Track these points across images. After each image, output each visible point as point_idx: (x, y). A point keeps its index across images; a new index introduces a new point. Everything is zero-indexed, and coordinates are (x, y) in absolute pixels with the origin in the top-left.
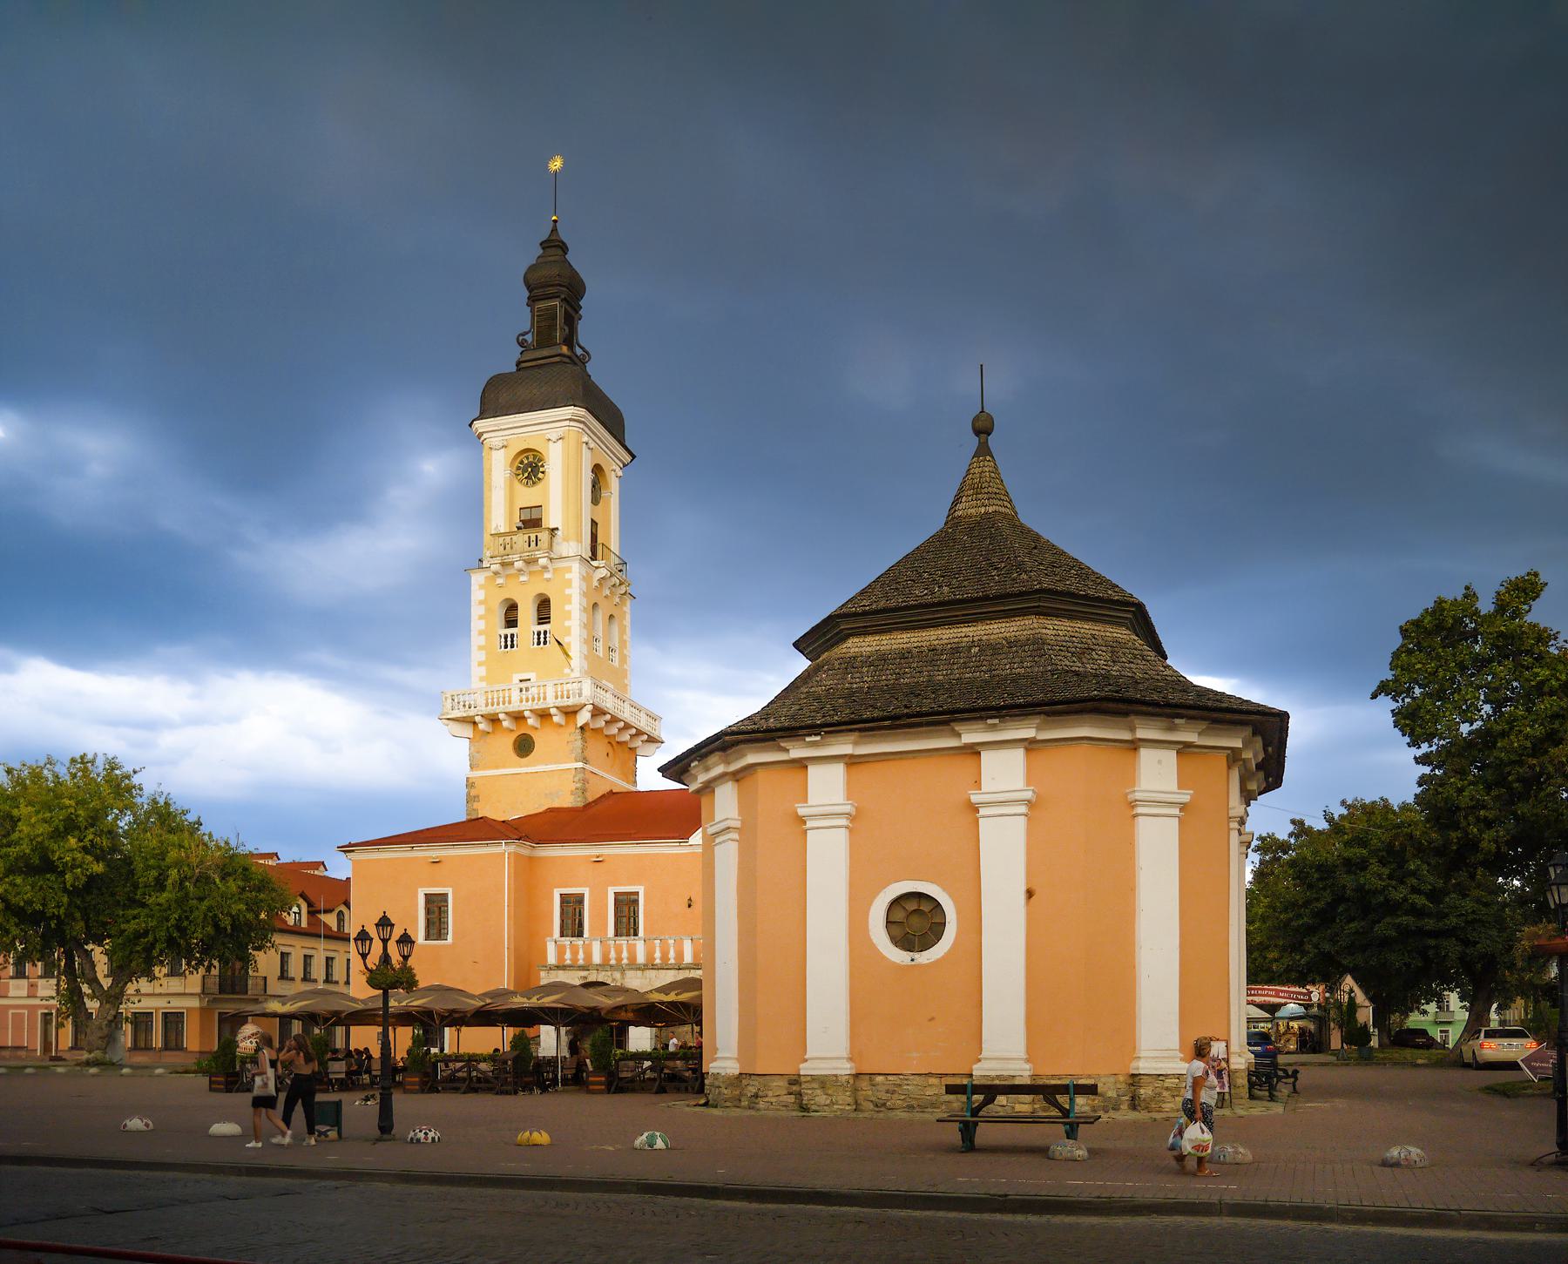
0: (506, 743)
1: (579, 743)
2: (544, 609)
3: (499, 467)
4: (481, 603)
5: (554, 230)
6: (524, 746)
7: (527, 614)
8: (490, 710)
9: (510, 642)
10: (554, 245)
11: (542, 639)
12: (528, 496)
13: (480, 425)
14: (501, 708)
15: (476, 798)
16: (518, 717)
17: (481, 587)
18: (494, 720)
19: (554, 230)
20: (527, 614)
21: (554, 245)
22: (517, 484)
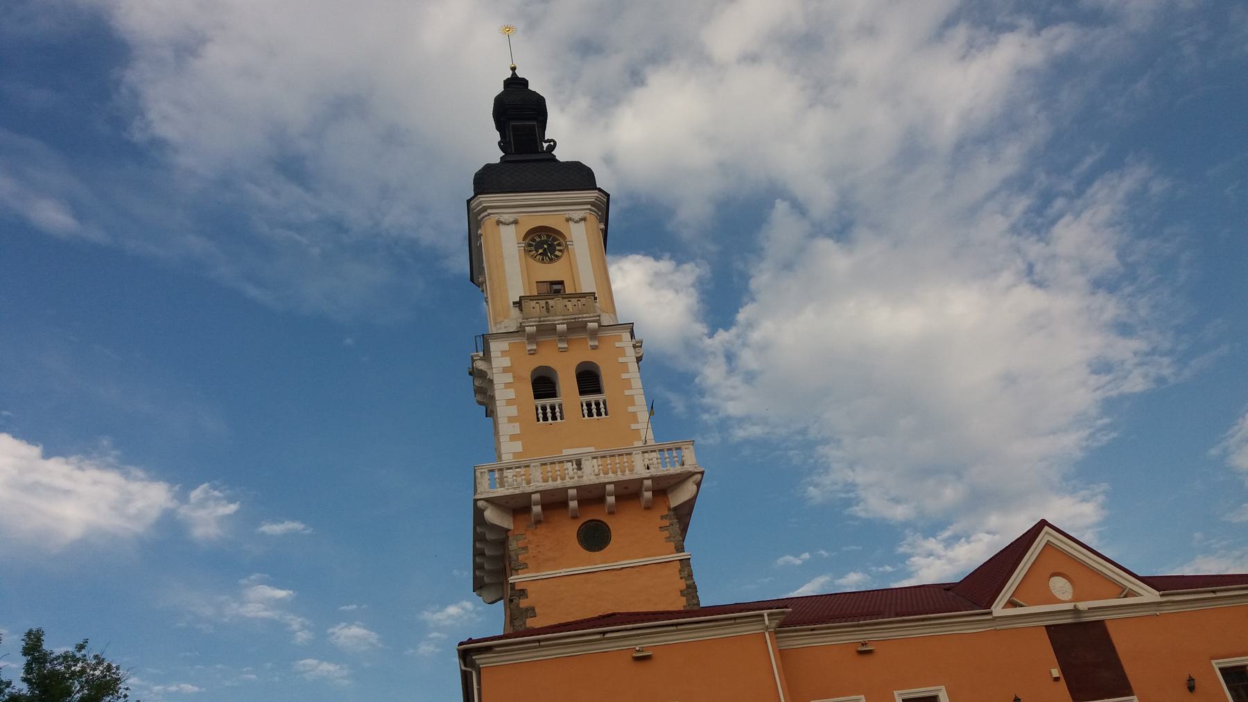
1: (676, 527)
2: (589, 380)
4: (506, 370)
5: (514, 74)
6: (595, 537)
7: (567, 384)
8: (551, 485)
11: (592, 410)
12: (551, 272)
13: (486, 199)
14: (568, 483)
15: (531, 611)
16: (592, 496)
17: (504, 353)
18: (555, 502)
19: (514, 74)
20: (567, 384)
22: (531, 261)
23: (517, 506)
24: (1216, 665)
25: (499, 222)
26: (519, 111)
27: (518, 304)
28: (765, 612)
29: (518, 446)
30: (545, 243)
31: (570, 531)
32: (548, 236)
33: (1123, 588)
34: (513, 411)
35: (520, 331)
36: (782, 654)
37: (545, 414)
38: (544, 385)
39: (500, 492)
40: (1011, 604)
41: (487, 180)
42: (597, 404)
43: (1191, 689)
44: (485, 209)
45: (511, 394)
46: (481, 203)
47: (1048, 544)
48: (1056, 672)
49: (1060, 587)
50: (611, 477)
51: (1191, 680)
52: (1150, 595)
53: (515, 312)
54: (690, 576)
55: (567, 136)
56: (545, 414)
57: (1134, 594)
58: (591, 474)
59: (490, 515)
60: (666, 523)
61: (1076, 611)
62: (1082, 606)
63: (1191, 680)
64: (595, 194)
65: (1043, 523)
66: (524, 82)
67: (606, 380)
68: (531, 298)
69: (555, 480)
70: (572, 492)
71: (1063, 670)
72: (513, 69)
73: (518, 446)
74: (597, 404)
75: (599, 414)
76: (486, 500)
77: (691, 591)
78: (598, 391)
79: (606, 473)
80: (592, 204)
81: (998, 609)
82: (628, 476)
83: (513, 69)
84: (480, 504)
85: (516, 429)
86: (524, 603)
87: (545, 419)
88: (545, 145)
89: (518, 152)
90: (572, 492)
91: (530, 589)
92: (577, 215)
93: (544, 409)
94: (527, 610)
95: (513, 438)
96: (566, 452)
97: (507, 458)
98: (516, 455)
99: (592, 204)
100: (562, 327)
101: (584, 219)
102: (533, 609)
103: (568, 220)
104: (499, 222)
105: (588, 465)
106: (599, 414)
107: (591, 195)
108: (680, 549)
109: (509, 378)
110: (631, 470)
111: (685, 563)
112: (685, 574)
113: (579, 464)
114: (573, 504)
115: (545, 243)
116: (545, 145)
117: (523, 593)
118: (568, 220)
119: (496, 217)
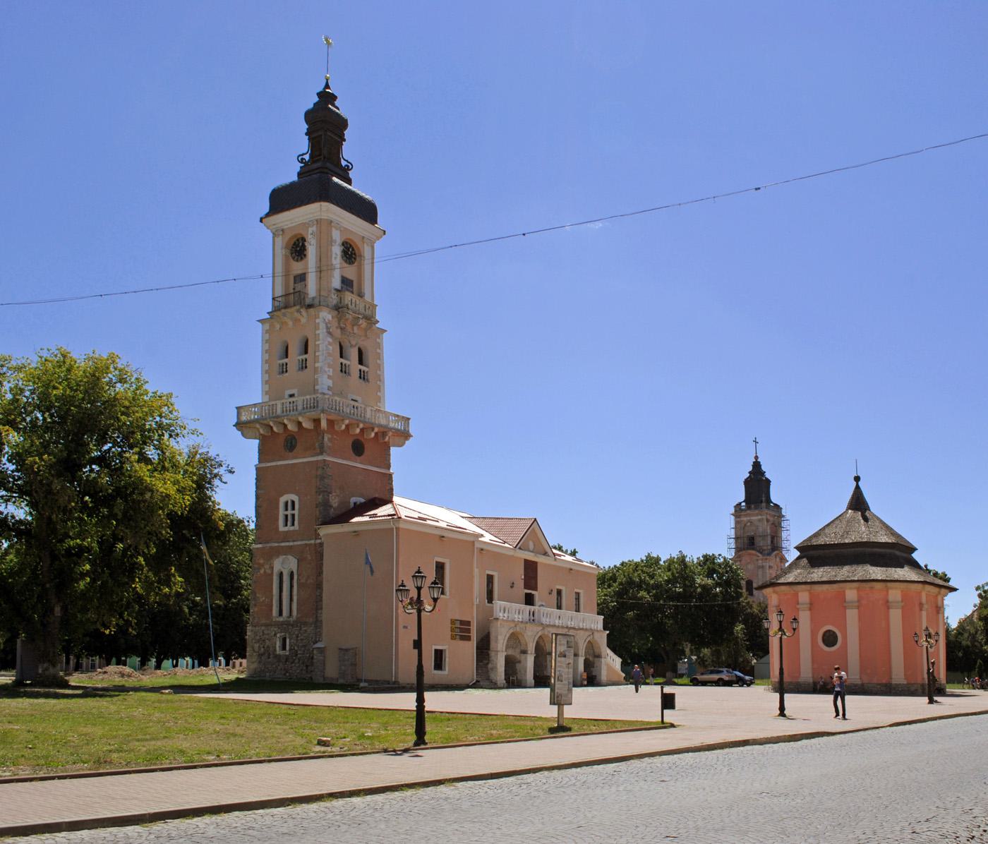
5: (327, 86)
10: (326, 97)
12: (350, 272)
19: (327, 86)
21: (326, 97)
29: (330, 383)
31: (349, 442)
66: (333, 98)
67: (369, 357)
73: (330, 383)
95: (329, 377)
98: (329, 388)
116: (344, 163)
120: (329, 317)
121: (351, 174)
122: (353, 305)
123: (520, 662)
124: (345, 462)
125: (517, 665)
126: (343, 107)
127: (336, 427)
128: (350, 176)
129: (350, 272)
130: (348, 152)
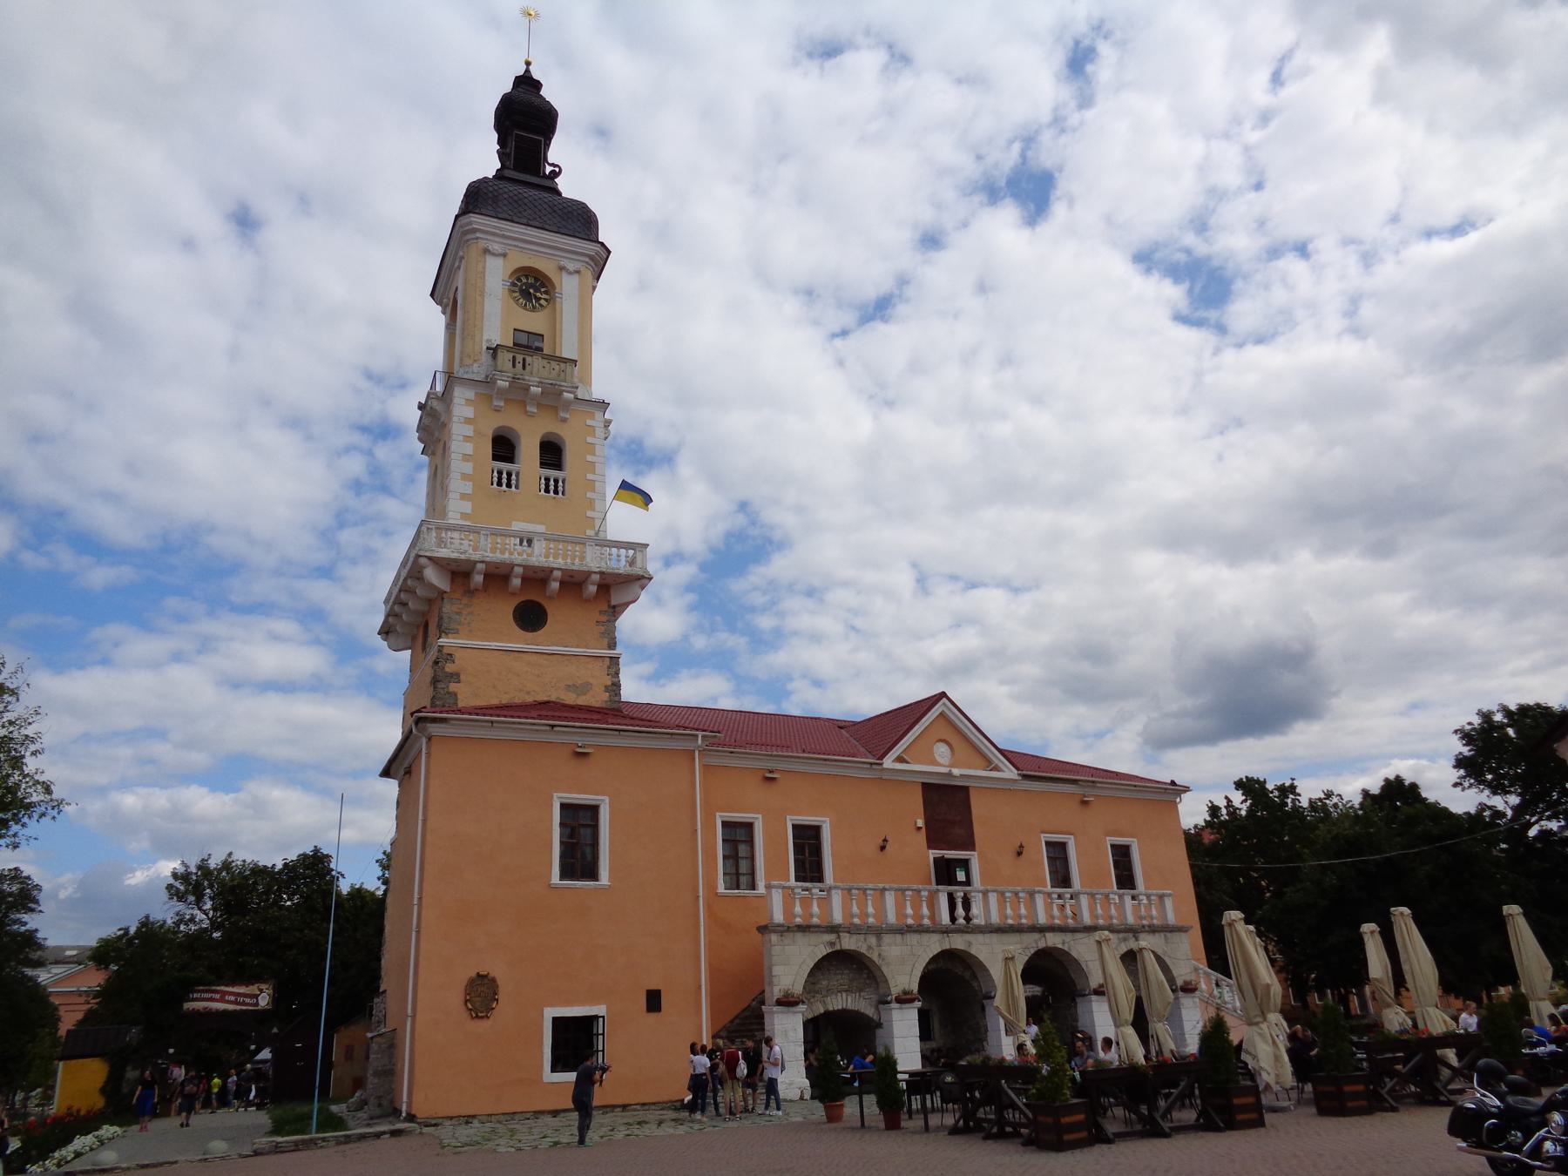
0: (505, 610)
2: (552, 453)
3: (495, 275)
4: (468, 421)
5: (527, 71)
6: (530, 617)
7: (529, 452)
8: (497, 557)
9: (506, 481)
10: (527, 83)
11: (553, 487)
12: (533, 321)
13: (476, 220)
14: (517, 559)
16: (537, 578)
19: (527, 71)
20: (529, 452)
21: (527, 83)
23: (459, 572)
24: (1044, 837)
25: (486, 251)
26: (525, 119)
27: (494, 351)
28: (700, 734)
29: (467, 507)
30: (532, 287)
31: (506, 609)
32: (536, 279)
33: (989, 762)
34: (468, 468)
35: (488, 382)
36: (706, 768)
37: (500, 479)
38: (504, 448)
39: (444, 553)
40: (900, 759)
41: (477, 197)
42: (556, 481)
43: (1019, 854)
44: (475, 231)
45: (469, 448)
46: (471, 223)
47: (942, 714)
48: (920, 823)
49: (941, 751)
50: (560, 562)
51: (1021, 846)
52: (1010, 773)
53: (485, 358)
54: (617, 674)
55: (574, 166)
56: (500, 479)
57: (996, 769)
58: (539, 555)
59: (431, 574)
60: (604, 618)
61: (950, 775)
62: (956, 772)
63: (1021, 846)
64: (598, 248)
65: (943, 695)
66: (537, 85)
67: (569, 457)
68: (508, 349)
69: (502, 553)
70: (518, 570)
71: (926, 823)
72: (528, 64)
73: (467, 507)
74: (556, 481)
75: (556, 492)
76: (430, 558)
77: (616, 687)
78: (558, 465)
79: (556, 557)
80: (590, 257)
81: (888, 762)
82: (577, 565)
83: (528, 64)
84: (423, 561)
85: (468, 488)
86: (449, 668)
87: (500, 484)
88: (548, 169)
89: (515, 169)
90: (518, 570)
91: (458, 655)
92: (571, 266)
93: (500, 473)
94: (452, 675)
95: (464, 497)
96: (517, 526)
97: (453, 518)
98: (464, 516)
99: (590, 257)
100: (536, 390)
101: (578, 272)
102: (458, 675)
103: (562, 268)
104: (486, 251)
105: (539, 546)
106: (556, 492)
107: (590, 247)
108: (612, 645)
109: (469, 430)
110: (582, 558)
111: (615, 661)
112: (612, 671)
113: (530, 542)
114: (516, 582)
115: (532, 287)
116: (548, 169)
117: (450, 657)
118: (562, 268)
119: (482, 244)
120: (470, 394)
121: (562, 183)
122: (519, 366)
123: (879, 1025)
124: (494, 645)
125: (879, 1032)
126: (550, 93)
127: (472, 586)
128: (561, 188)
129: (533, 321)
130: (558, 152)
